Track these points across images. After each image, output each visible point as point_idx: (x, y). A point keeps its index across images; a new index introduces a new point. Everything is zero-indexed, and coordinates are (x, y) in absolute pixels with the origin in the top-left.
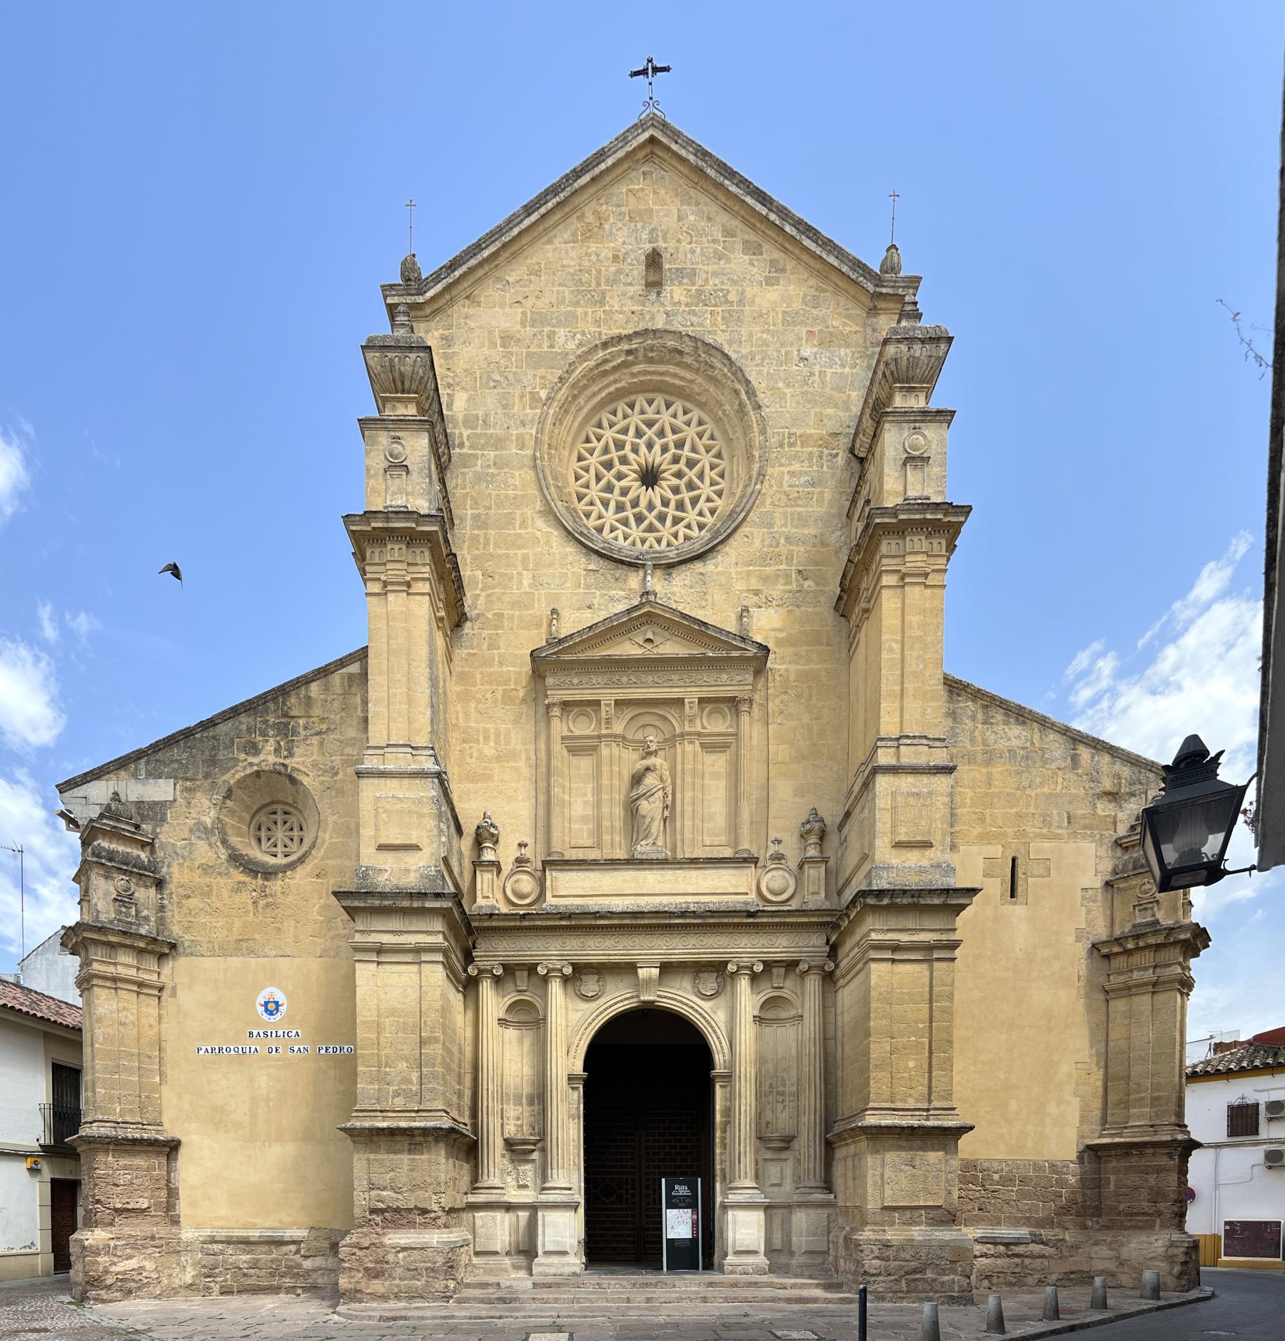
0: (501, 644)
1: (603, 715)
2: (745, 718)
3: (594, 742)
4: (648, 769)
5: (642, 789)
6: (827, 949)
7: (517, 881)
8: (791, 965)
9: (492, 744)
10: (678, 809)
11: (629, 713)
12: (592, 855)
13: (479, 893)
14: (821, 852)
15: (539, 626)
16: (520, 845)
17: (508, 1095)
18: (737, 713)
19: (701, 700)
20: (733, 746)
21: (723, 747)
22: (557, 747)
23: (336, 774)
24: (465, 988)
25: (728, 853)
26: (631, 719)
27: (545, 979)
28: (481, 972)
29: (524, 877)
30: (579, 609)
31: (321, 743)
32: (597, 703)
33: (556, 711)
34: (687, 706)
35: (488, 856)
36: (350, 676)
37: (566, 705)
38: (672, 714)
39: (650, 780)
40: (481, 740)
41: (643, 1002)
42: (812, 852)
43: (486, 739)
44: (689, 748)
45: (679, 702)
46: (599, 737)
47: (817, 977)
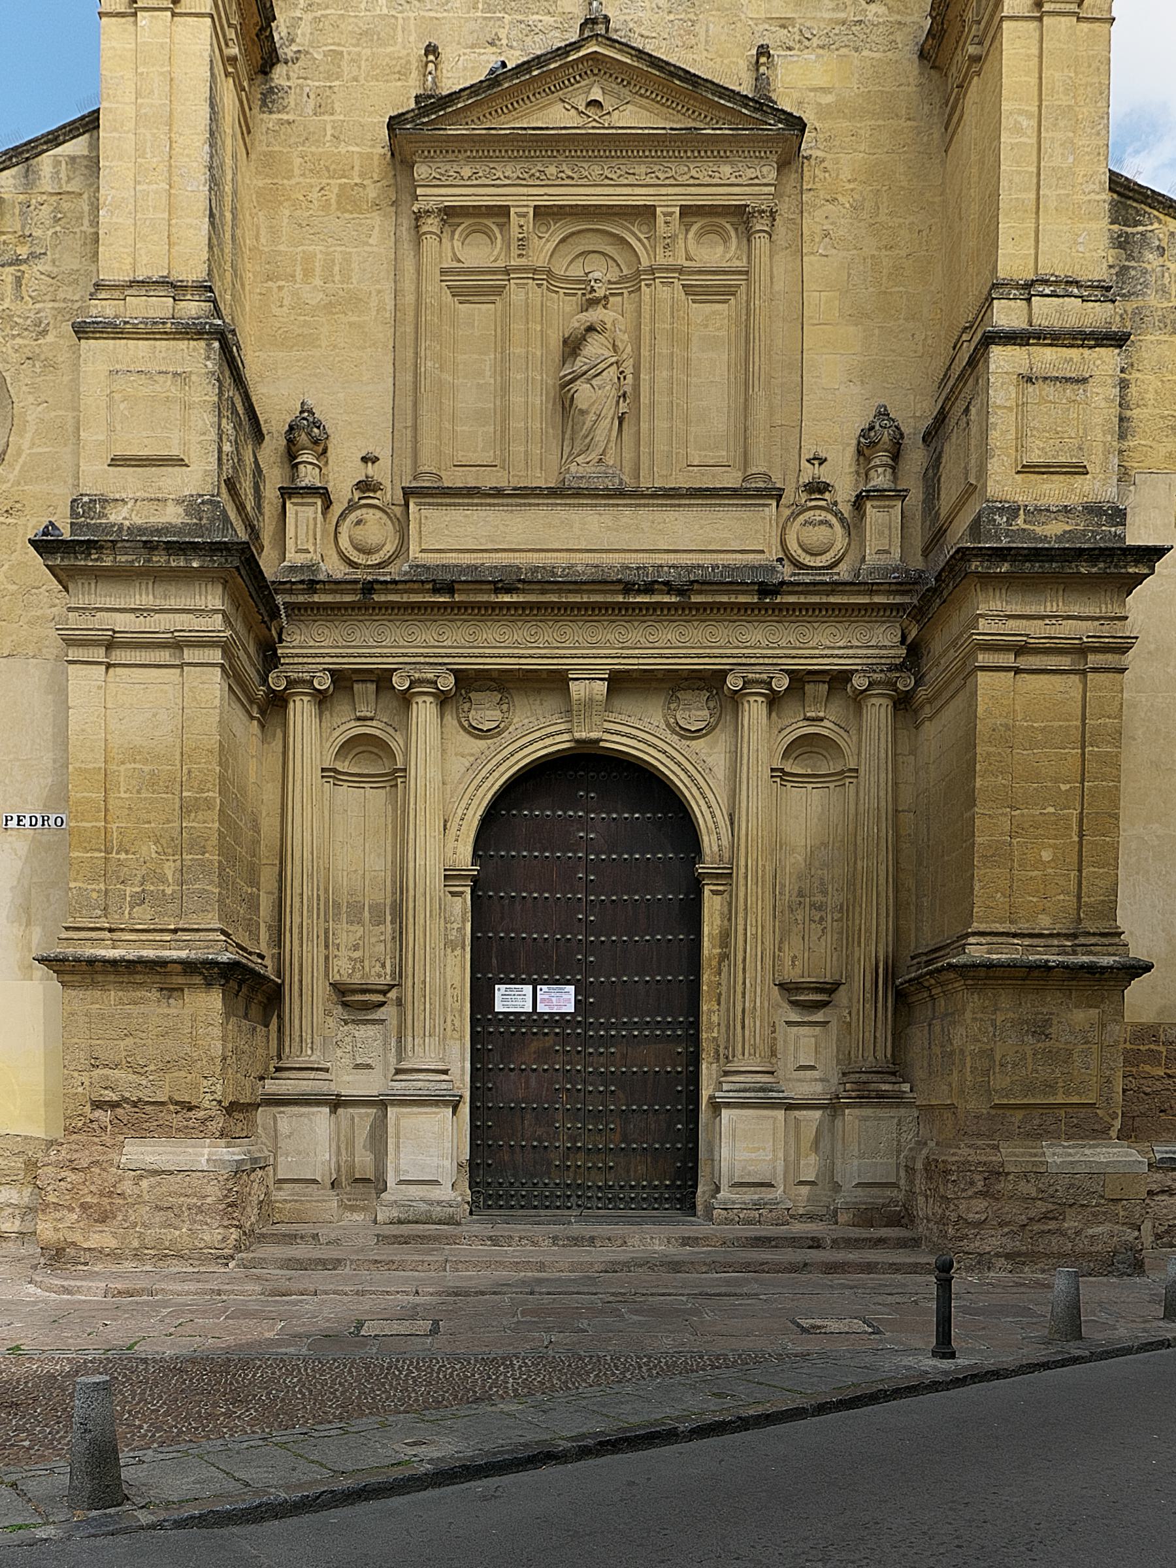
0: (337, 106)
1: (515, 231)
2: (761, 243)
3: (498, 280)
4: (591, 329)
5: (579, 364)
6: (903, 652)
7: (359, 522)
8: (838, 680)
9: (318, 282)
10: (644, 400)
11: (559, 230)
12: (489, 480)
13: (290, 544)
14: (895, 478)
15: (403, 74)
16: (365, 459)
17: (337, 905)
18: (748, 235)
19: (685, 211)
20: (743, 289)
21: (725, 293)
22: (434, 288)
23: (44, 332)
24: (263, 712)
25: (731, 479)
26: (563, 241)
27: (406, 699)
28: (291, 683)
29: (371, 515)
30: (473, 46)
31: (18, 281)
32: (502, 212)
33: (431, 224)
34: (660, 219)
35: (308, 476)
36: (73, 159)
37: (450, 214)
38: (634, 235)
39: (594, 348)
40: (299, 276)
41: (577, 741)
42: (880, 479)
43: (308, 273)
44: (664, 292)
45: (647, 213)
46: (507, 271)
47: (885, 701)
